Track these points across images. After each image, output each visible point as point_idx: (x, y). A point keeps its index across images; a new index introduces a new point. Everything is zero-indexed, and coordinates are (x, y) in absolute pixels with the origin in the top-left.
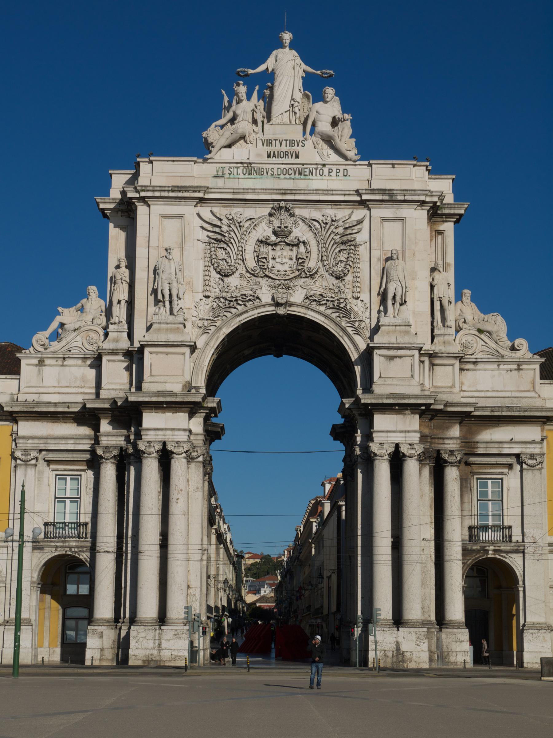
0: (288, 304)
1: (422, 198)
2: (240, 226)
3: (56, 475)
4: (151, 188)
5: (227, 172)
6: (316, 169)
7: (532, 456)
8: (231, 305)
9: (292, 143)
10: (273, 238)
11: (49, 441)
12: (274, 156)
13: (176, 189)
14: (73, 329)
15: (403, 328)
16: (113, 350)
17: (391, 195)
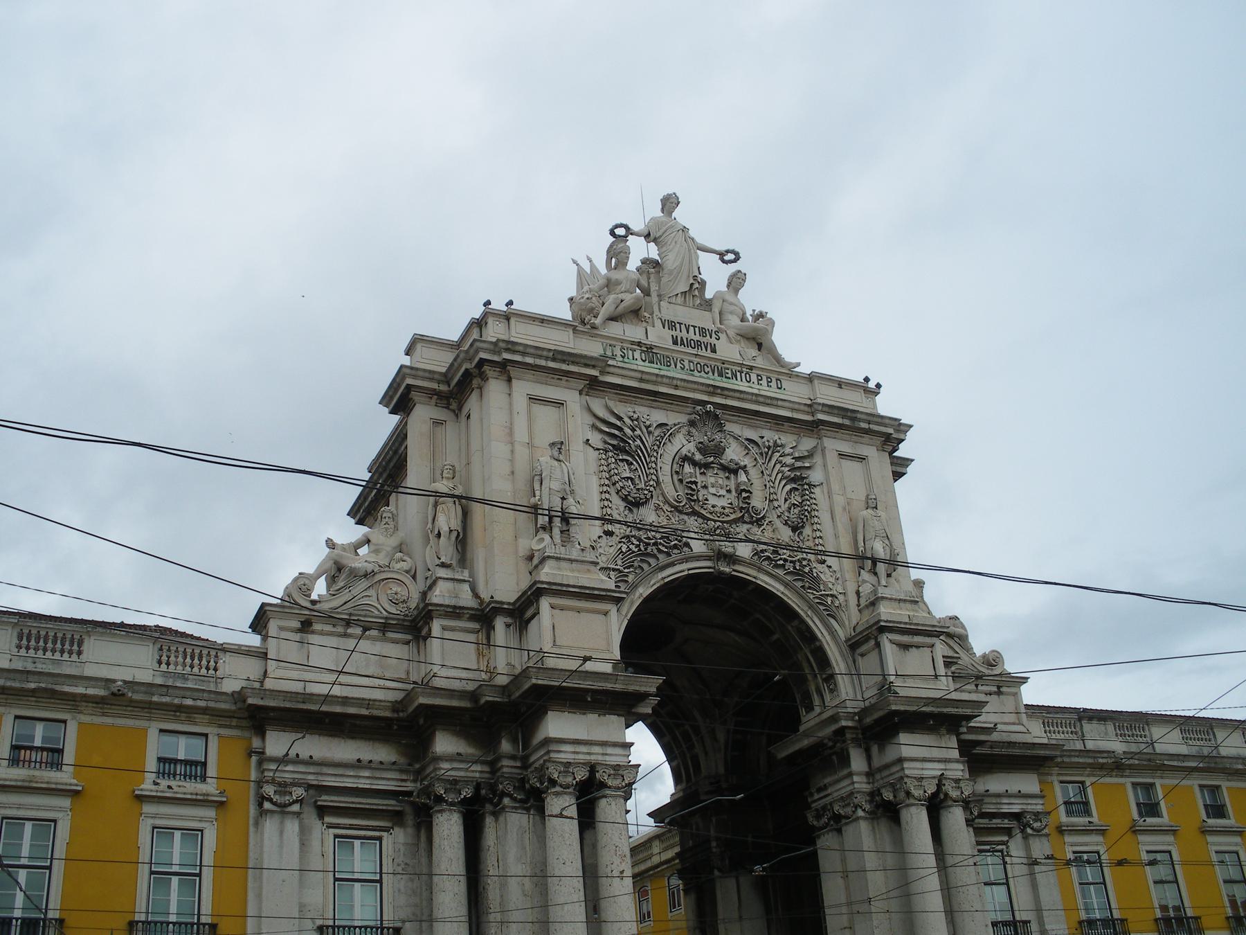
0: (732, 559)
1: (891, 431)
2: (650, 433)
3: (336, 836)
4: (521, 348)
5: (619, 353)
6: (741, 372)
7: (1037, 816)
8: (649, 550)
9: (703, 331)
10: (698, 457)
11: (325, 770)
12: (683, 343)
13: (560, 357)
14: (362, 573)
15: (908, 605)
16: (455, 607)
17: (853, 419)
